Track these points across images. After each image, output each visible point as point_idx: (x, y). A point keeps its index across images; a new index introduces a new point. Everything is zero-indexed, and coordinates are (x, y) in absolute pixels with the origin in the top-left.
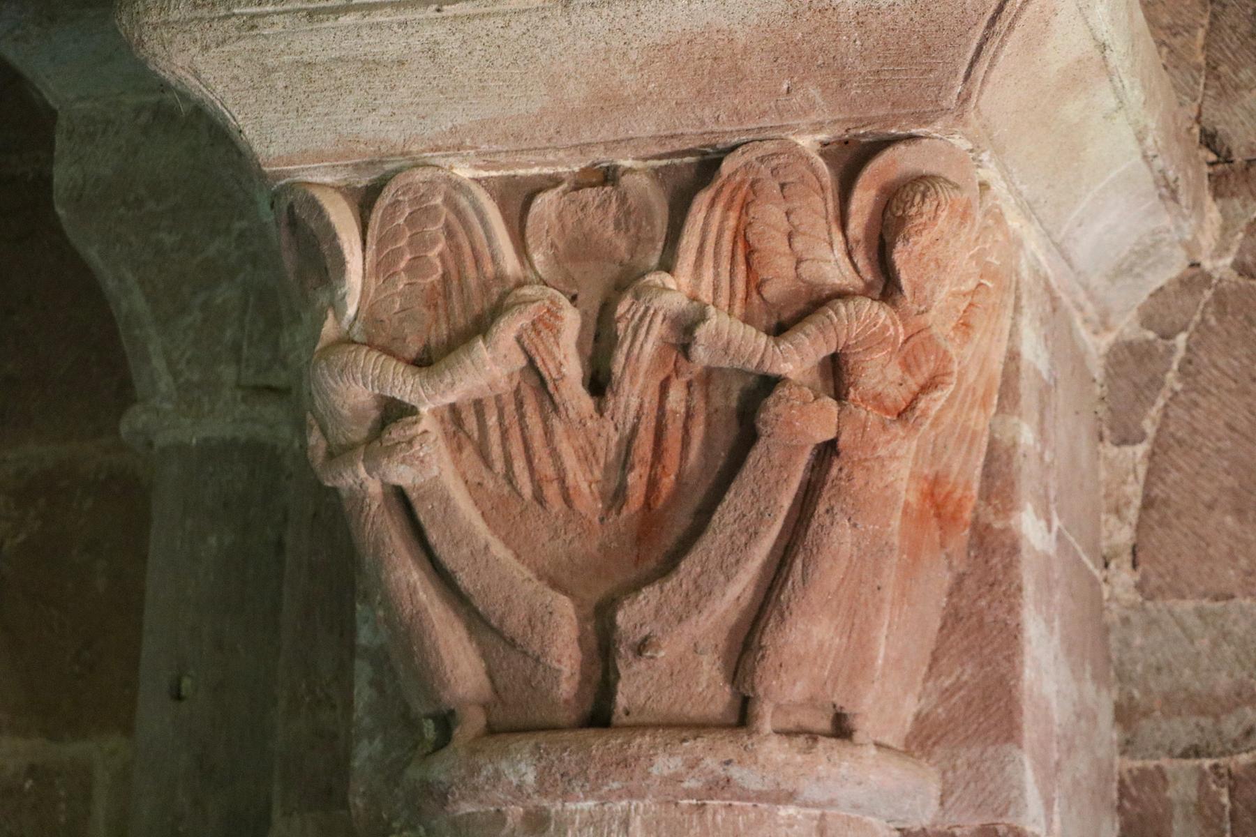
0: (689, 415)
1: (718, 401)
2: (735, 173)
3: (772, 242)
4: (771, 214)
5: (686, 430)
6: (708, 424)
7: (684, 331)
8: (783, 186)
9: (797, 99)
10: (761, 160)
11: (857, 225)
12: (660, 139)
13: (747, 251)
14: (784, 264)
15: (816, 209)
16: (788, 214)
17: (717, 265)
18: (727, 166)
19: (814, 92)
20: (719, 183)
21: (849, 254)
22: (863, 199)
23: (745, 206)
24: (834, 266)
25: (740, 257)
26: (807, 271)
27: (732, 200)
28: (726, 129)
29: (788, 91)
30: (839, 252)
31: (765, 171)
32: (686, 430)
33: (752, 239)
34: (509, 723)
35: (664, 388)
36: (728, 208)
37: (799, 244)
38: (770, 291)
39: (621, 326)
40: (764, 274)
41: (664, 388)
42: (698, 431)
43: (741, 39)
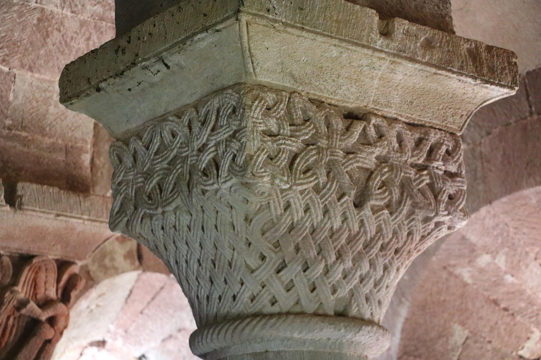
0: (13, 326)
1: (21, 323)
2: (36, 263)
3: (41, 284)
4: (42, 276)
5: (12, 330)
6: (17, 329)
7: (23, 304)
8: (46, 269)
9: (54, 248)
10: (43, 261)
11: (62, 283)
12: (17, 249)
13: (35, 285)
14: (43, 290)
15: (52, 276)
16: (46, 277)
17: (28, 286)
18: (35, 261)
19: (59, 247)
20: (31, 265)
21: (57, 290)
22: (65, 277)
23: (37, 273)
24: (52, 293)
25: (33, 286)
26: (47, 293)
27: (34, 270)
28: (34, 250)
29: (54, 245)
30: (54, 290)
31: (43, 265)
32: (12, 330)
33: (37, 281)
35: (8, 318)
36: (33, 272)
37: (47, 285)
38: (39, 296)
39: (5, 300)
40: (38, 291)
41: (8, 318)
42: (14, 331)
43: (50, 230)
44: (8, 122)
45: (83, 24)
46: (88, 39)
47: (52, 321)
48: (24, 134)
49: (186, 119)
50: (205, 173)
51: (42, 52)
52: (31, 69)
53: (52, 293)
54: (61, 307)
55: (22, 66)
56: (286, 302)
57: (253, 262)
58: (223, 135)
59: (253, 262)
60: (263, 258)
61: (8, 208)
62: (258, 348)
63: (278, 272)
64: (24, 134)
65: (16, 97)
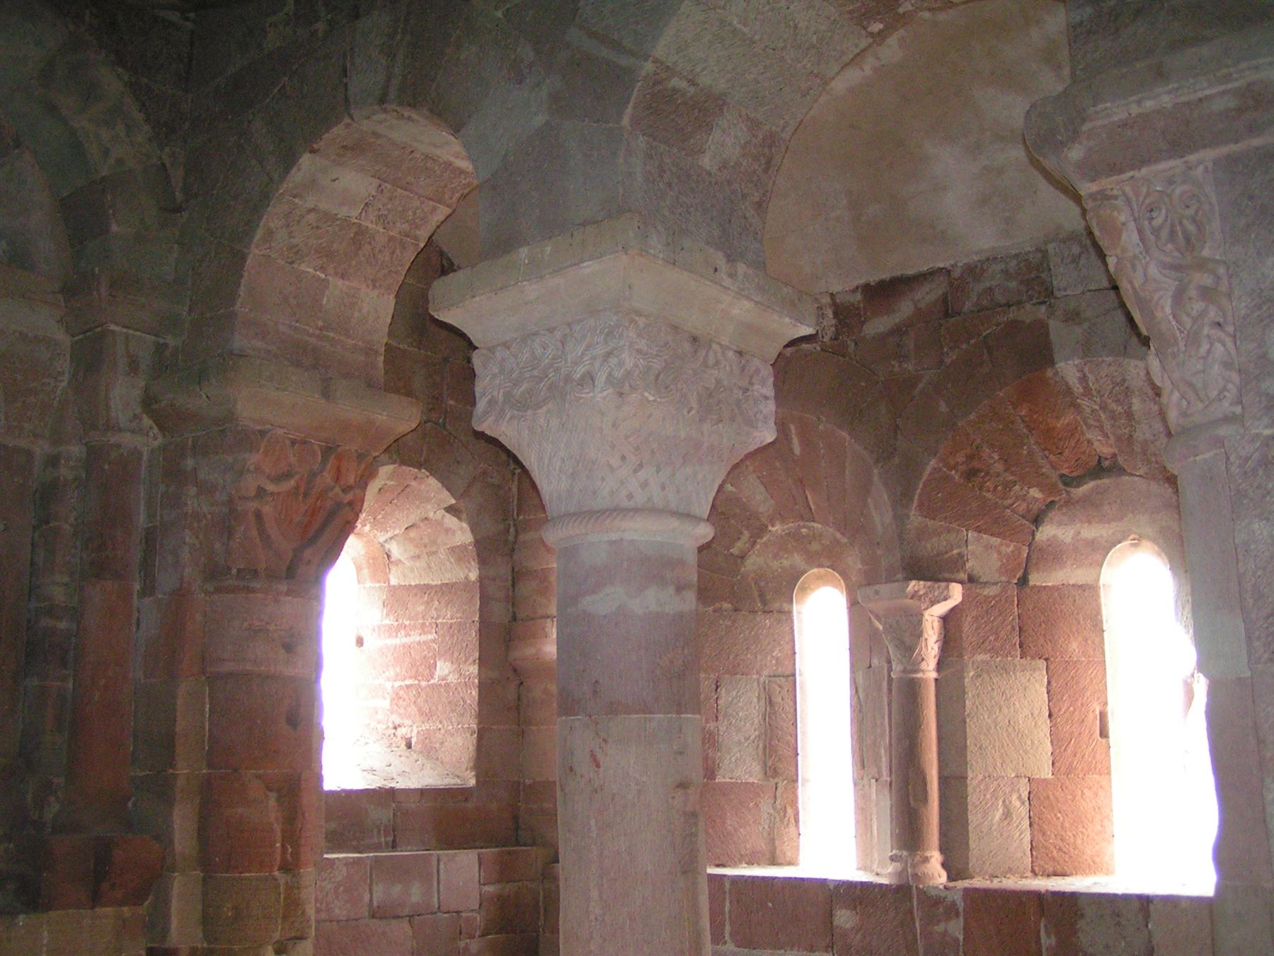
24: (351, 480)
34: (272, 576)
44: (320, 323)
45: (391, 239)
46: (393, 253)
47: (350, 504)
48: (332, 334)
49: (558, 334)
50: (581, 383)
51: (354, 263)
52: (343, 277)
53: (351, 480)
54: (358, 491)
55: (336, 274)
56: (640, 498)
57: (615, 462)
58: (600, 351)
59: (615, 462)
60: (623, 458)
61: (323, 401)
62: (614, 536)
63: (635, 471)
64: (332, 334)
65: (328, 301)
